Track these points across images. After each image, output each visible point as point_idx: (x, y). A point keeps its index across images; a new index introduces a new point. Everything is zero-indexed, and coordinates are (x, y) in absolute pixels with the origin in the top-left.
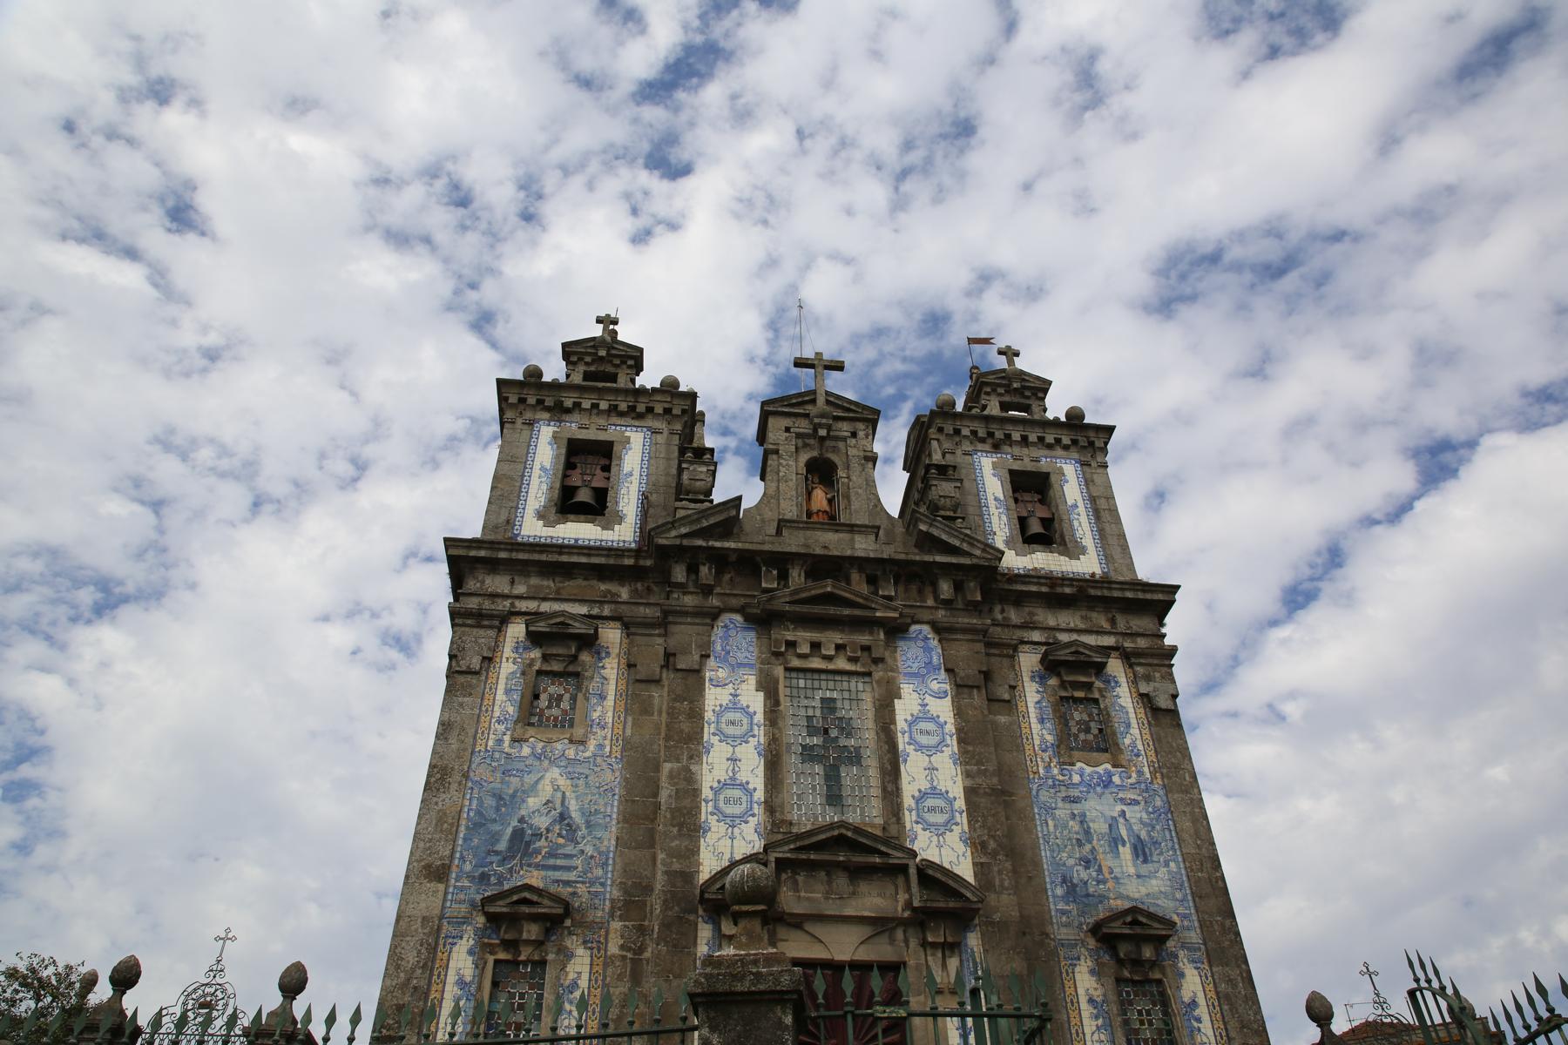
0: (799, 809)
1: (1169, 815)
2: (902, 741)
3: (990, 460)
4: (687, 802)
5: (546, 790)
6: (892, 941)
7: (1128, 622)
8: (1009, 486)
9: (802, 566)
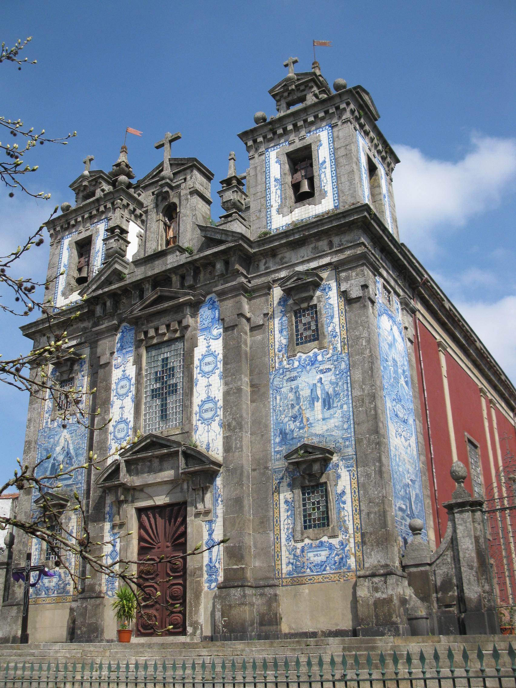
0: (149, 427)
1: (349, 373)
3: (276, 151)
5: (62, 442)
6: (182, 490)
7: (341, 241)
9: (149, 283)
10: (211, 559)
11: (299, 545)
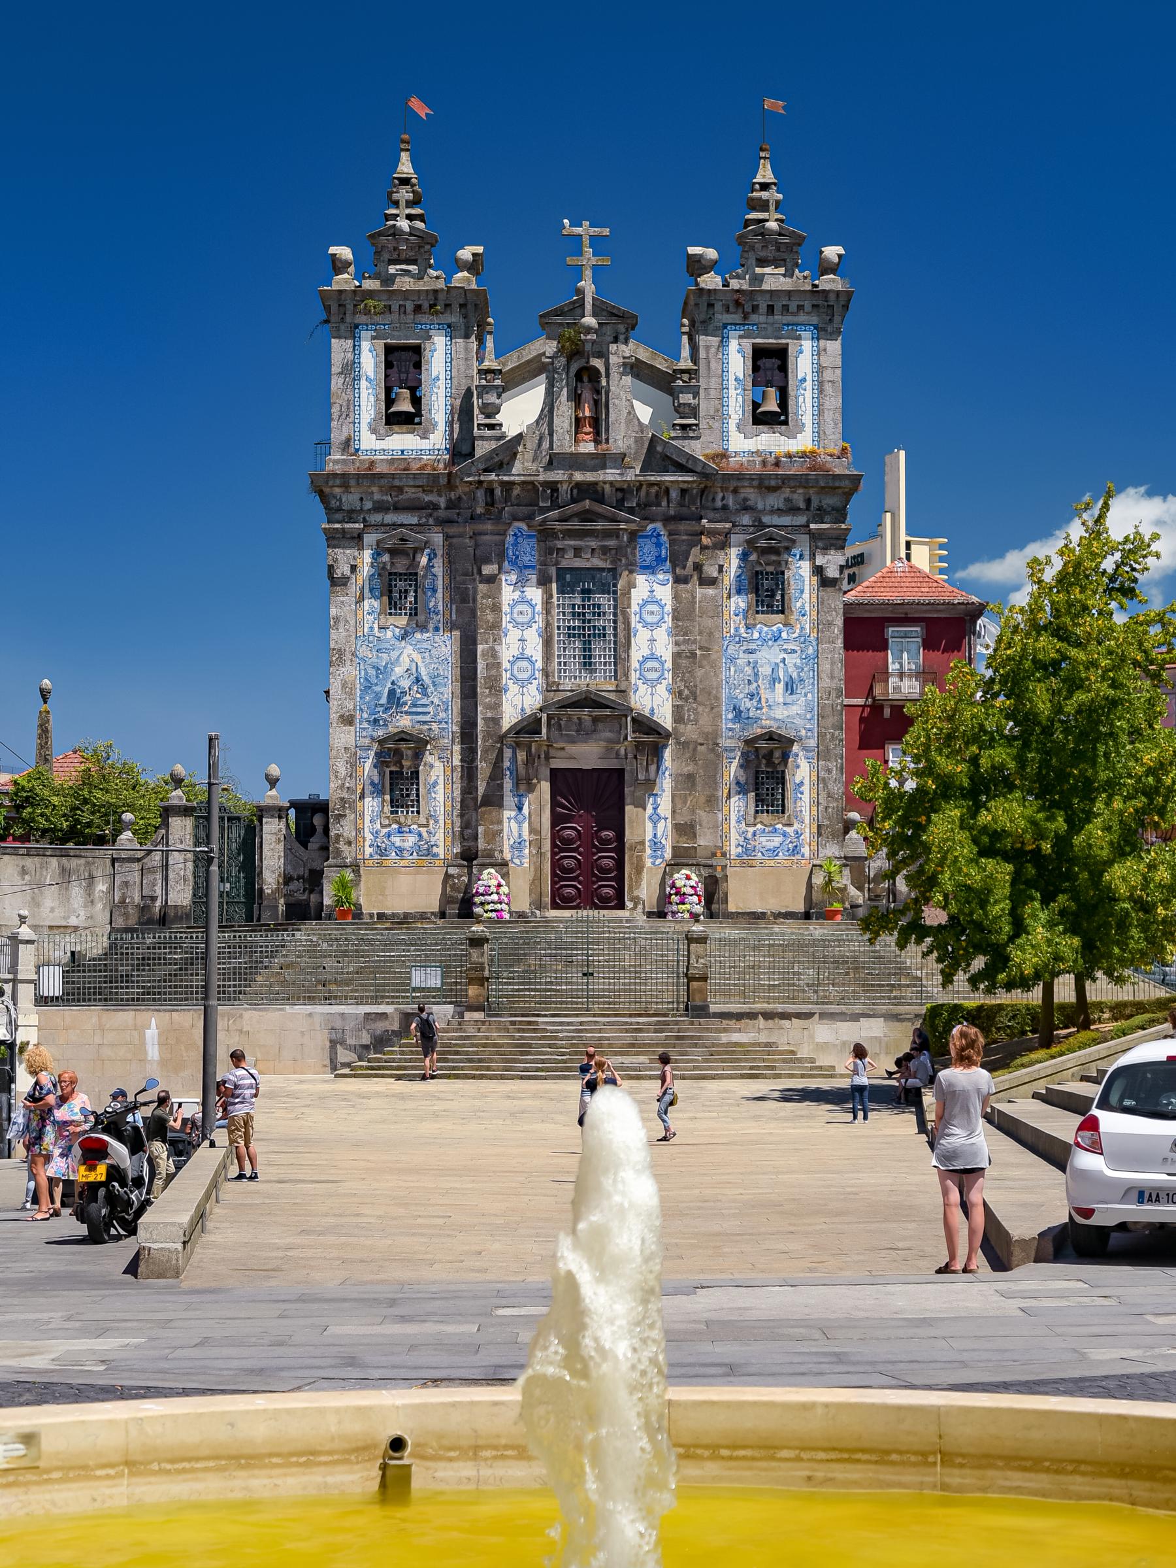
2: (634, 620)
4: (494, 672)
5: (405, 662)
8: (750, 363)
10: (655, 835)
11: (751, 830)
